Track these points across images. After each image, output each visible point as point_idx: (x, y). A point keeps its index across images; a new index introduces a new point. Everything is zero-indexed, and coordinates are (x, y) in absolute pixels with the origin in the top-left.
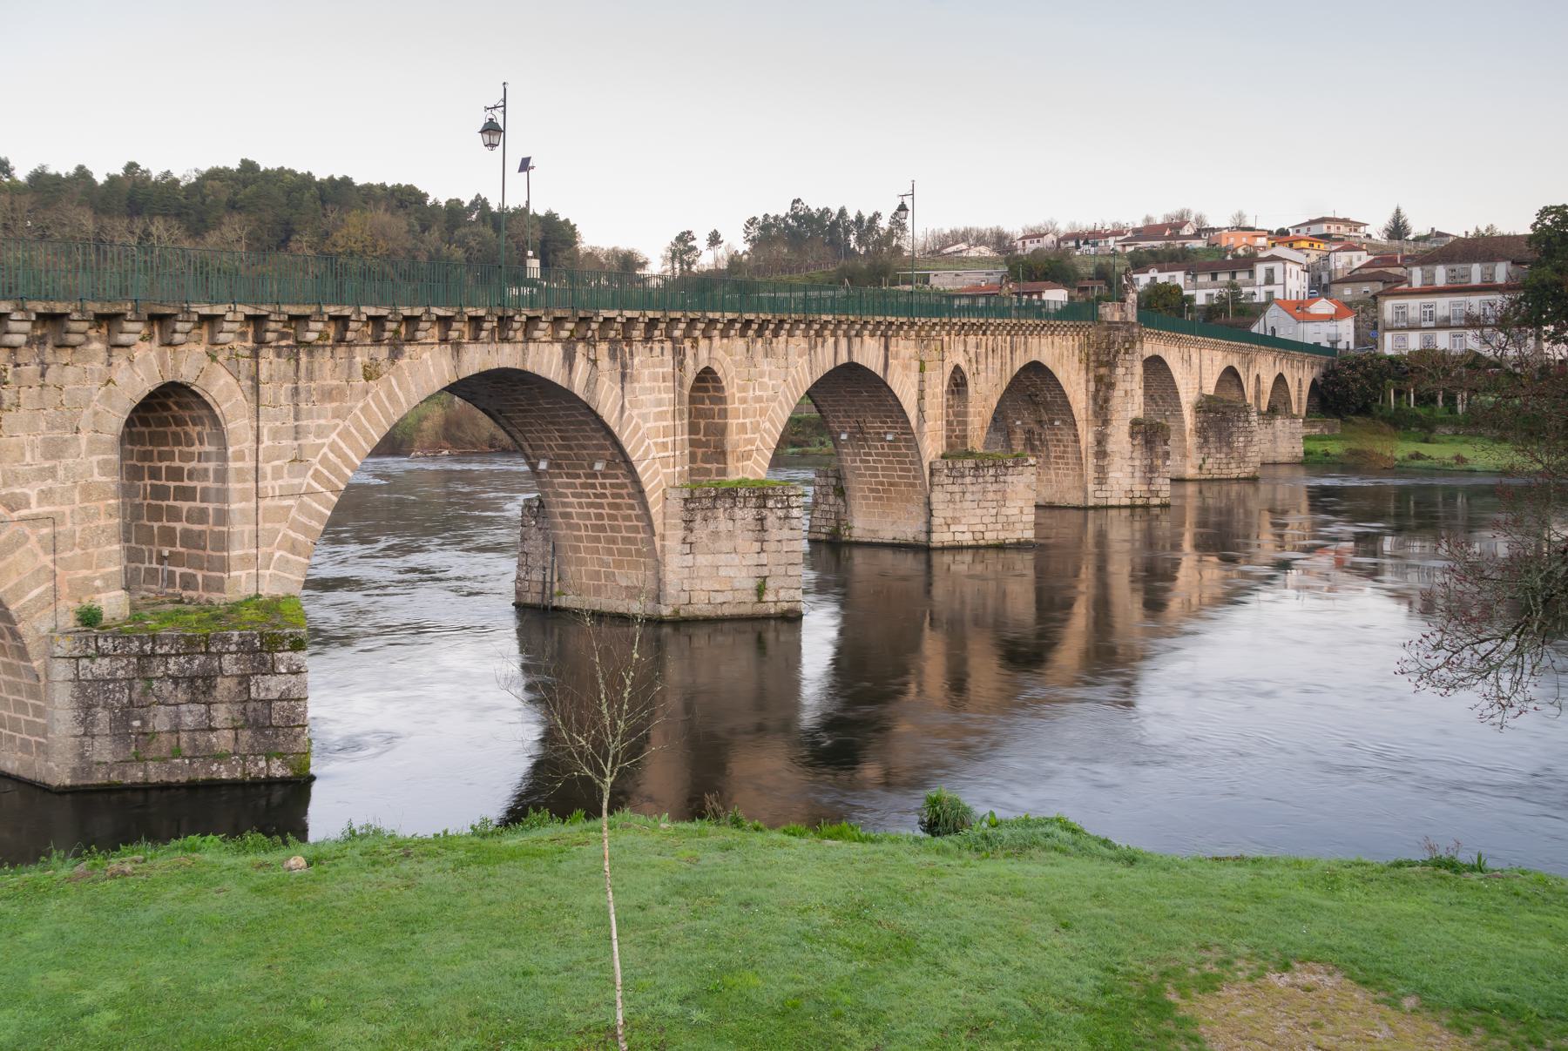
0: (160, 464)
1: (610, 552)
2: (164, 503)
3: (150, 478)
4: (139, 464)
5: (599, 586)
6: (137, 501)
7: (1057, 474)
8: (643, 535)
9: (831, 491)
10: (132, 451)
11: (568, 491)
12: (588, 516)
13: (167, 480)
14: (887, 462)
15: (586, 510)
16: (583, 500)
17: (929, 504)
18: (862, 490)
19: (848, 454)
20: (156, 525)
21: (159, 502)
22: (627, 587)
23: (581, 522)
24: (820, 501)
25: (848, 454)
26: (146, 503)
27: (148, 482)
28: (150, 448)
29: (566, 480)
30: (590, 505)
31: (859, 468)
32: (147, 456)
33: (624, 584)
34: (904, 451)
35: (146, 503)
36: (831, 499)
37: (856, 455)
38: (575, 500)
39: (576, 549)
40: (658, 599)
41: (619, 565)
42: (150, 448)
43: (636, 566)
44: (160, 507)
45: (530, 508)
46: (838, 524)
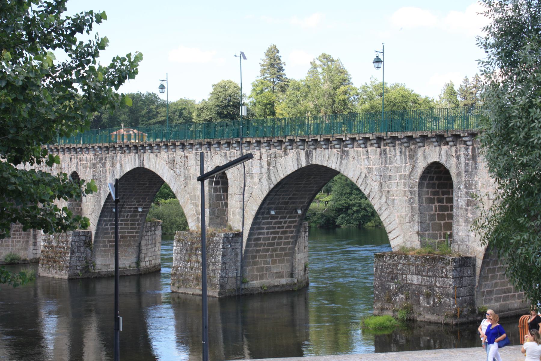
0: (442, 197)
1: (271, 256)
2: (446, 213)
3: (438, 203)
4: (432, 197)
5: (263, 275)
6: (432, 213)
7: (13, 242)
8: (291, 246)
9: (82, 244)
10: (428, 191)
11: (265, 226)
12: (268, 239)
13: (446, 203)
14: (125, 224)
15: (269, 236)
16: (270, 231)
17: (139, 245)
18: (104, 242)
19: (105, 221)
20: (442, 222)
21: (443, 213)
22: (277, 273)
23: (263, 242)
24: (76, 251)
25: (105, 221)
26: (436, 213)
27: (438, 204)
28: (438, 190)
29: (269, 220)
30: (272, 233)
31: (107, 229)
32: (436, 193)
33: (275, 272)
34: (138, 217)
35: (436, 213)
36: (82, 249)
37: (110, 221)
38: (266, 231)
39: (255, 257)
40: (292, 275)
41: (274, 262)
42: (438, 190)
43: (281, 261)
44: (444, 215)
45: (228, 238)
46: (87, 263)
